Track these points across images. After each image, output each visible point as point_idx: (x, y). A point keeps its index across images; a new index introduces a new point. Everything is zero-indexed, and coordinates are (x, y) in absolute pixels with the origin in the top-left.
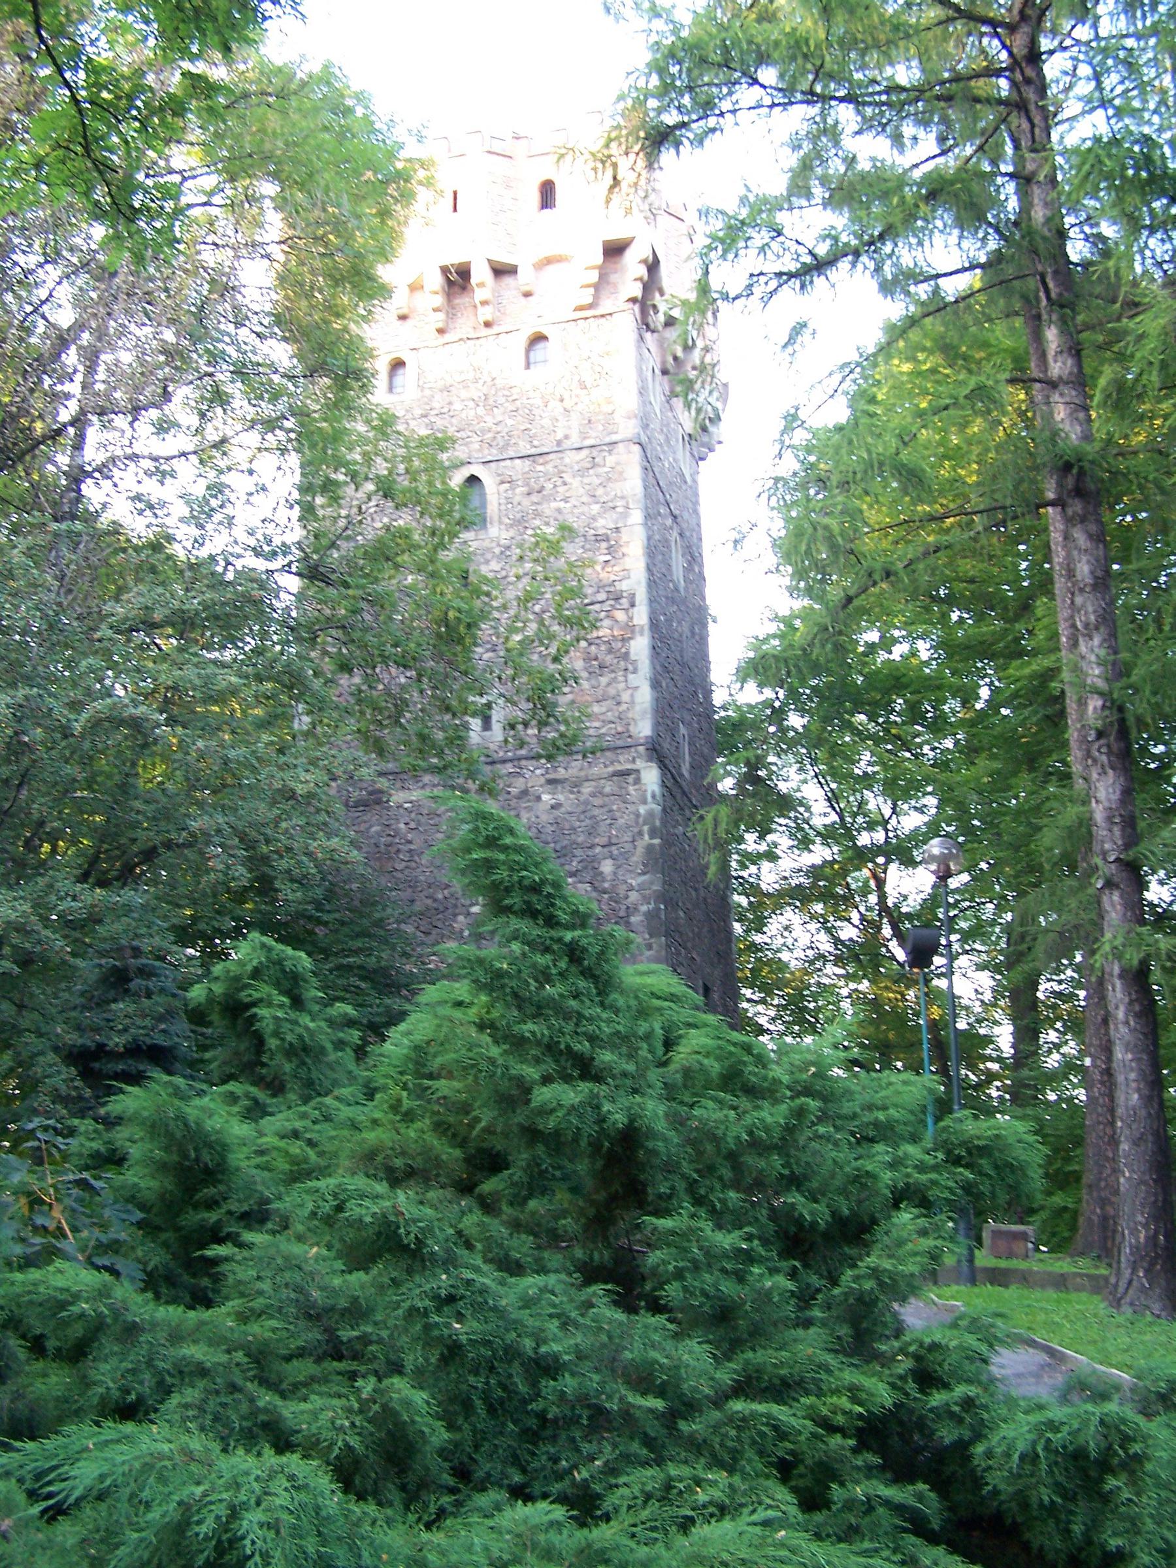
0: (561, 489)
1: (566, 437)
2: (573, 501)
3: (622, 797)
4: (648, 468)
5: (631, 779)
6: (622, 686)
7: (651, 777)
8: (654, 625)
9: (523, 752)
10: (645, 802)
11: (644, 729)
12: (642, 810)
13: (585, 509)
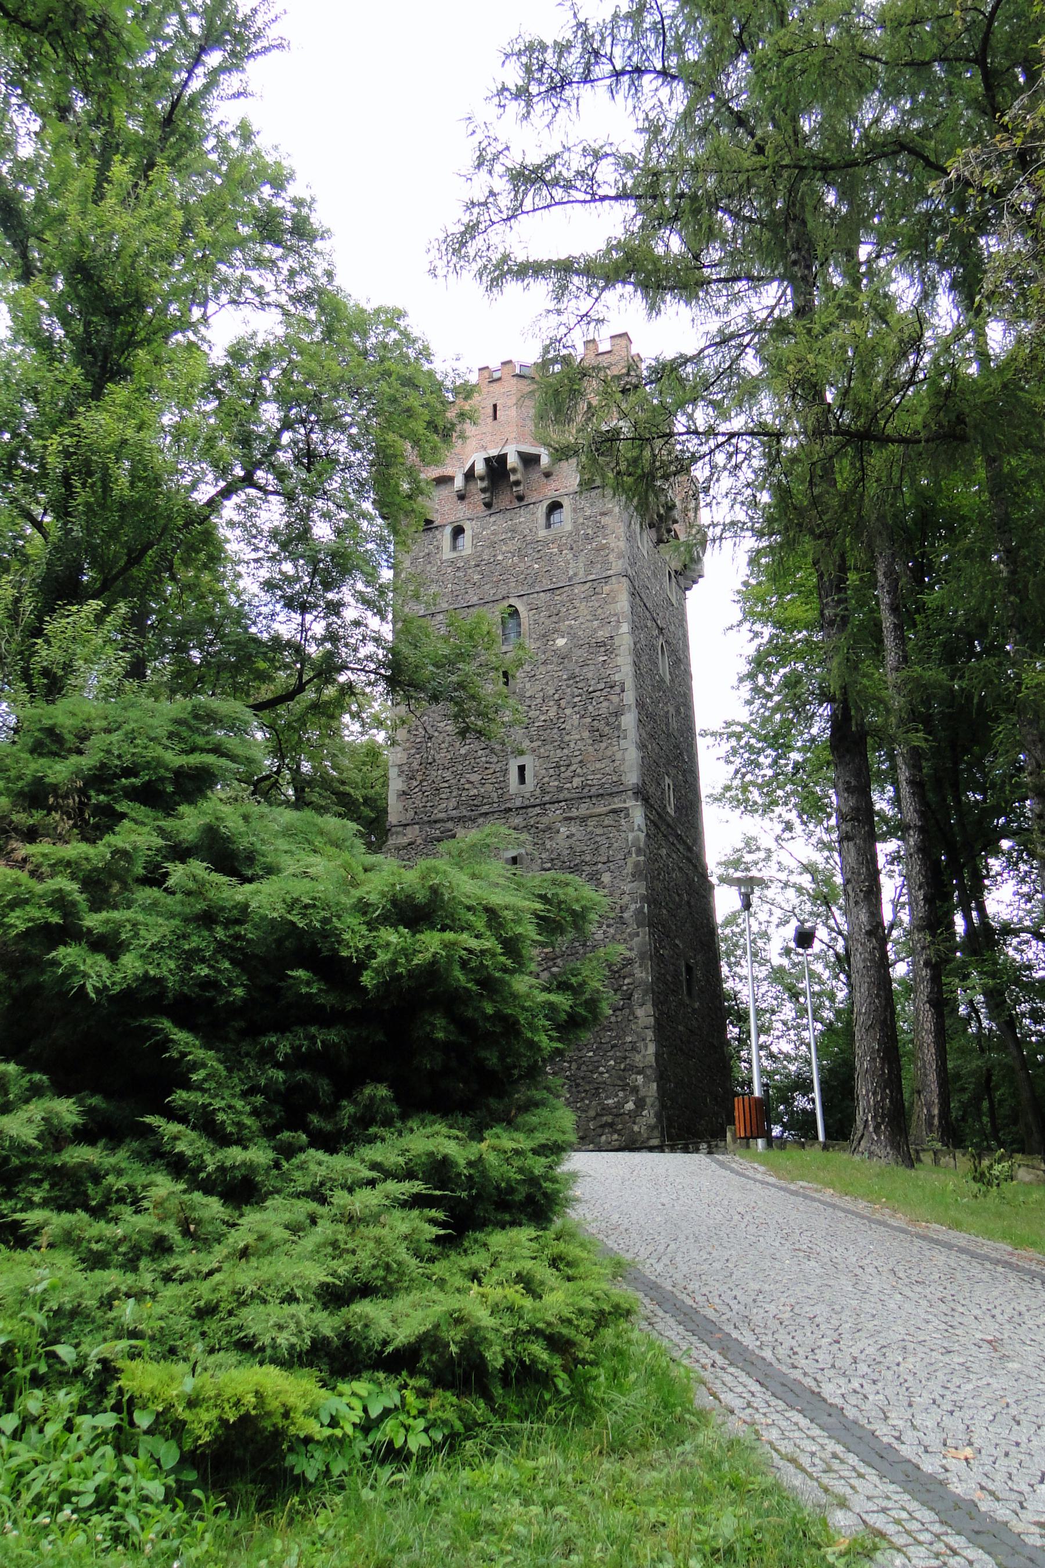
4: (634, 594)
7: (638, 815)
8: (640, 705)
9: (547, 798)
11: (632, 778)
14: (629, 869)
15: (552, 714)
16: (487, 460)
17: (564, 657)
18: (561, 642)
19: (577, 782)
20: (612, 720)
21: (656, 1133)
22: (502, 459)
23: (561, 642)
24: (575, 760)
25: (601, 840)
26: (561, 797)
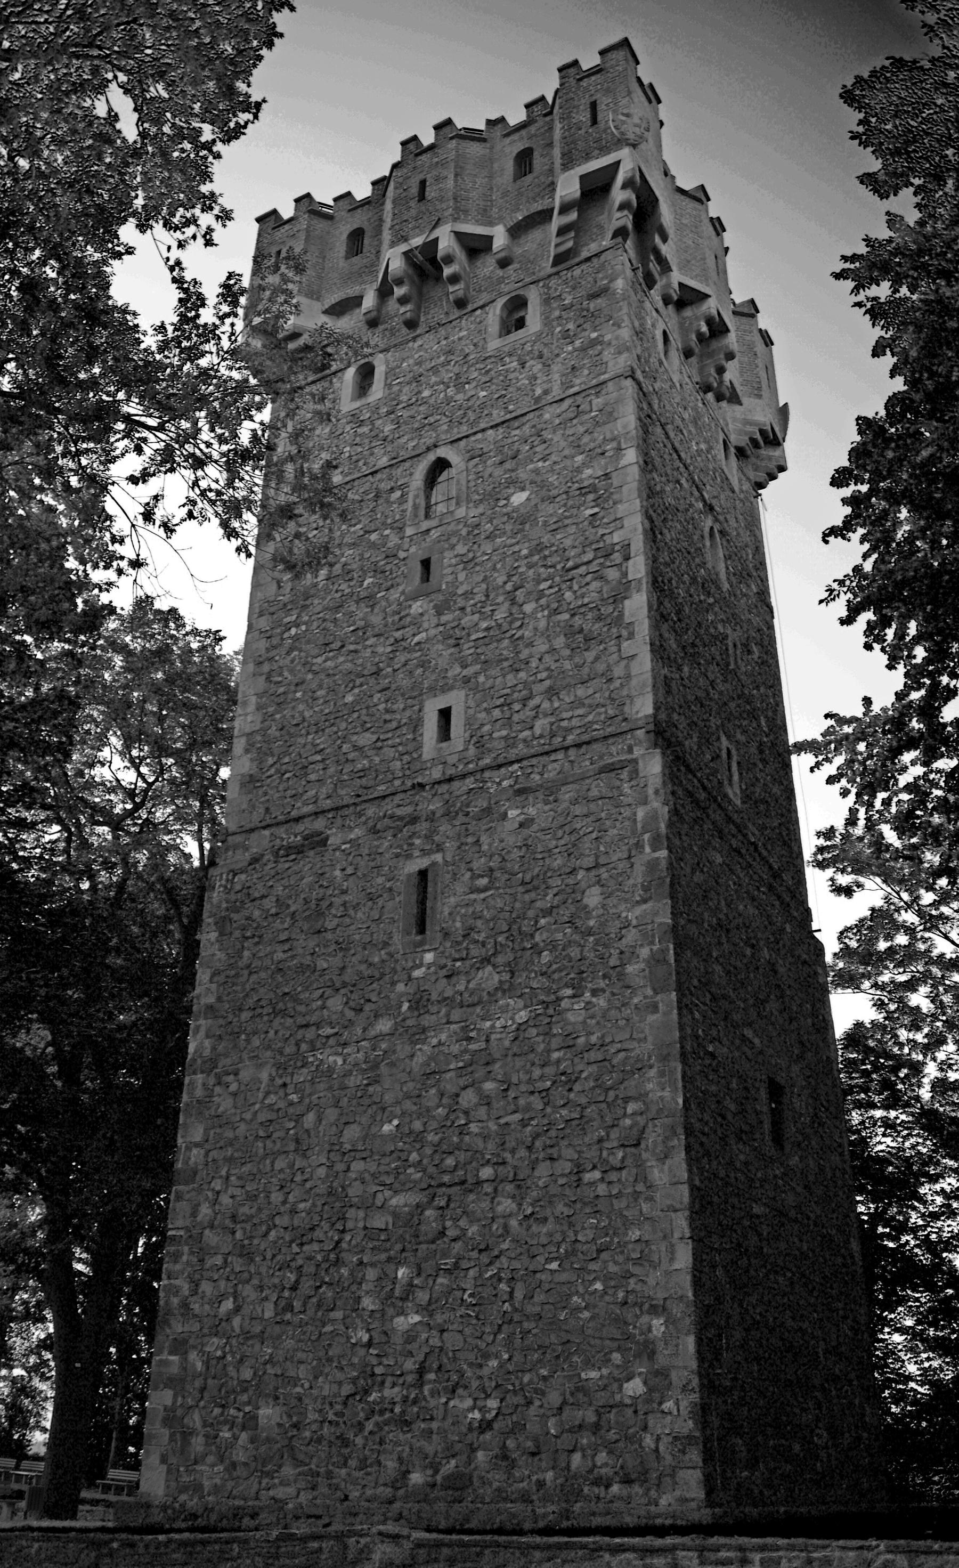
1: (546, 392)
2: (554, 458)
3: (614, 799)
5: (625, 775)
6: (615, 656)
8: (658, 583)
9: (487, 761)
10: (645, 802)
11: (644, 707)
12: (641, 813)
13: (568, 462)
14: (639, 875)
15: (500, 615)
17: (523, 519)
18: (519, 498)
19: (540, 725)
20: (607, 610)
21: (695, 1455)
23: (519, 498)
24: (537, 688)
26: (513, 754)
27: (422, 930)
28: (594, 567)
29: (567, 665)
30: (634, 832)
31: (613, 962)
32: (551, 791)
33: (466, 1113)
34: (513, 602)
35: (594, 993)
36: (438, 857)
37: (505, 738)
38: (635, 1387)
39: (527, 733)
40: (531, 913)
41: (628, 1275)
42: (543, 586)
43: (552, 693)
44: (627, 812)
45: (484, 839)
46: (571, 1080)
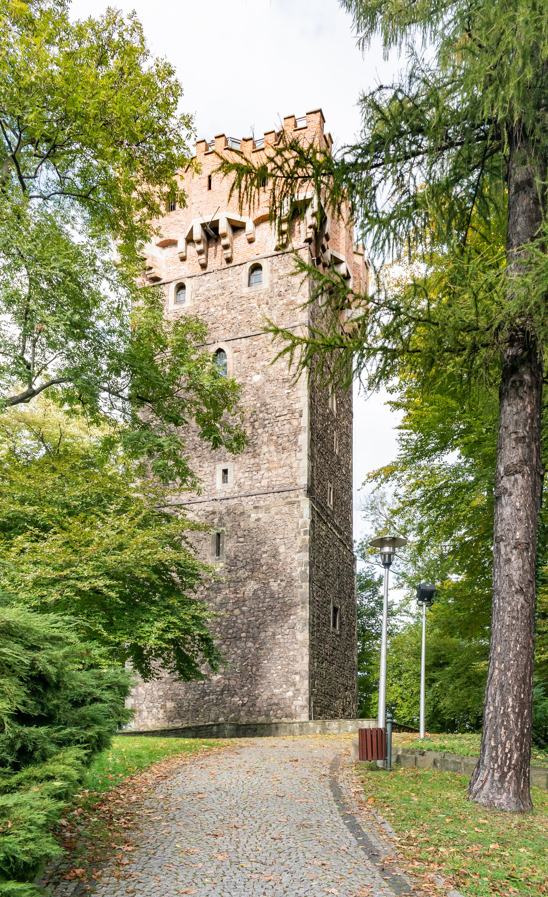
0: (266, 354)
5: (295, 506)
7: (305, 504)
9: (242, 493)
11: (303, 480)
12: (301, 521)
14: (299, 543)
16: (203, 225)
19: (264, 482)
21: (306, 710)
22: (214, 225)
25: (280, 523)
27: (218, 554)
28: (287, 417)
29: (275, 459)
30: (297, 527)
31: (288, 571)
32: (267, 509)
33: (236, 616)
34: (254, 427)
35: (281, 581)
36: (224, 529)
37: (250, 485)
38: (290, 694)
39: (258, 485)
40: (259, 552)
41: (289, 664)
42: (266, 422)
43: (269, 470)
44: (295, 520)
45: (242, 524)
46: (272, 608)
